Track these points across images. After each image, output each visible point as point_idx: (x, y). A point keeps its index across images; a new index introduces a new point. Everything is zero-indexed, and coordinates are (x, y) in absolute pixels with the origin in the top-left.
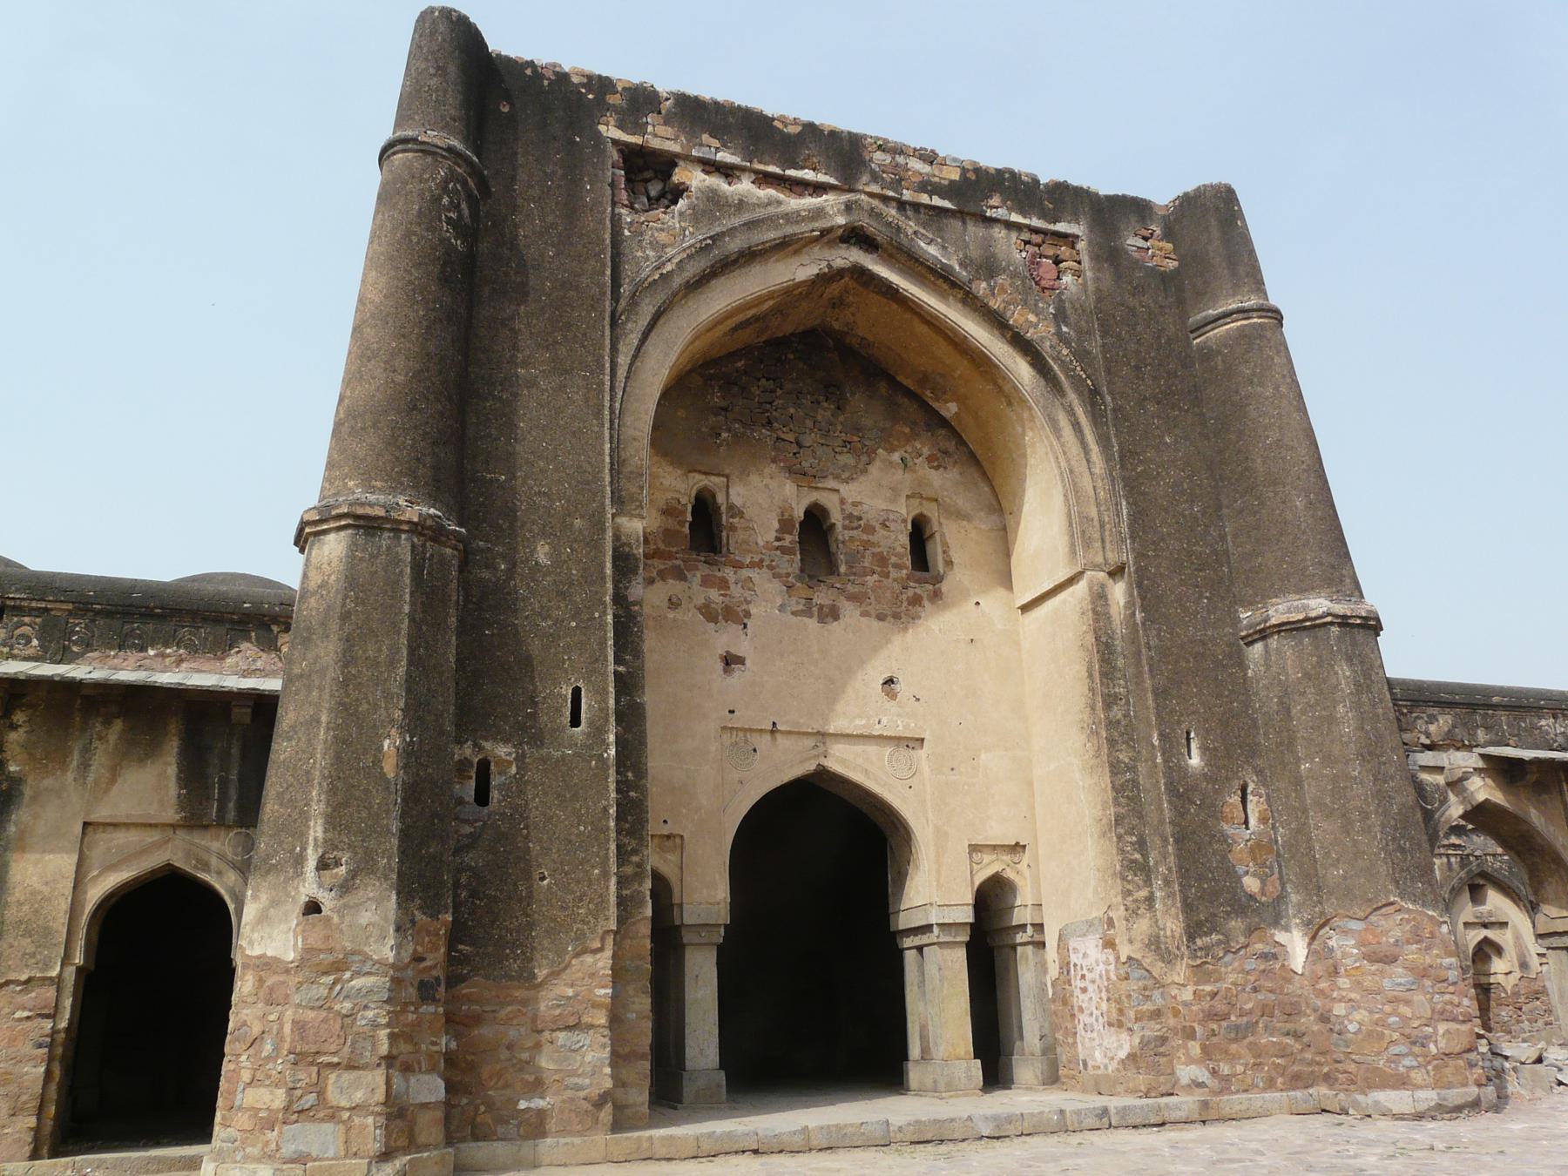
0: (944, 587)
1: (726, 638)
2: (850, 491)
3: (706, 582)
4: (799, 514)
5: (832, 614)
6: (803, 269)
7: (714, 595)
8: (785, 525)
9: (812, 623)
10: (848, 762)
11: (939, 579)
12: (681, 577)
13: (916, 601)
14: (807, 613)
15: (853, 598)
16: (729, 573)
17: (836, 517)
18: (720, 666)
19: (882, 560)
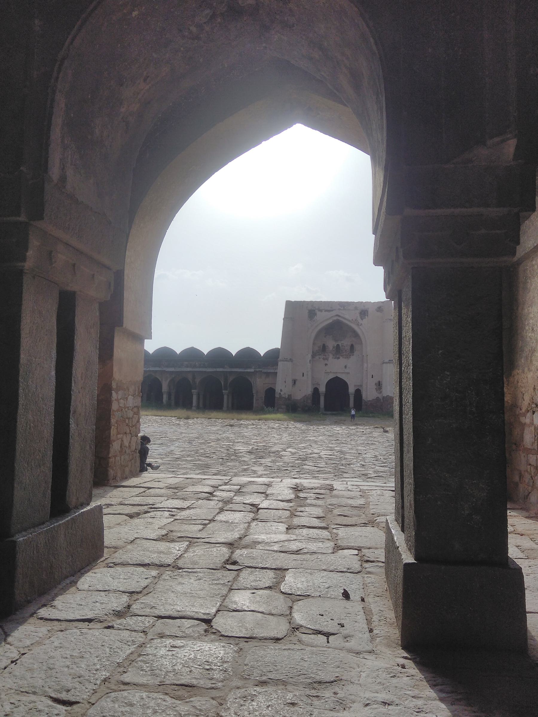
0: (354, 354)
1: (326, 362)
2: (342, 342)
3: (324, 355)
4: (336, 345)
5: (339, 358)
6: (331, 321)
7: (324, 357)
8: (334, 347)
9: (336, 359)
10: (340, 376)
11: (354, 352)
12: (320, 355)
13: (350, 355)
14: (335, 358)
15: (341, 356)
16: (326, 354)
17: (340, 346)
18: (325, 365)
19: (346, 351)
